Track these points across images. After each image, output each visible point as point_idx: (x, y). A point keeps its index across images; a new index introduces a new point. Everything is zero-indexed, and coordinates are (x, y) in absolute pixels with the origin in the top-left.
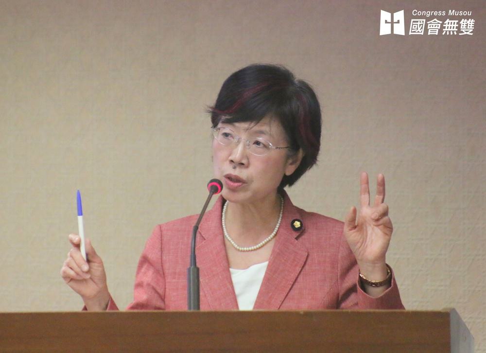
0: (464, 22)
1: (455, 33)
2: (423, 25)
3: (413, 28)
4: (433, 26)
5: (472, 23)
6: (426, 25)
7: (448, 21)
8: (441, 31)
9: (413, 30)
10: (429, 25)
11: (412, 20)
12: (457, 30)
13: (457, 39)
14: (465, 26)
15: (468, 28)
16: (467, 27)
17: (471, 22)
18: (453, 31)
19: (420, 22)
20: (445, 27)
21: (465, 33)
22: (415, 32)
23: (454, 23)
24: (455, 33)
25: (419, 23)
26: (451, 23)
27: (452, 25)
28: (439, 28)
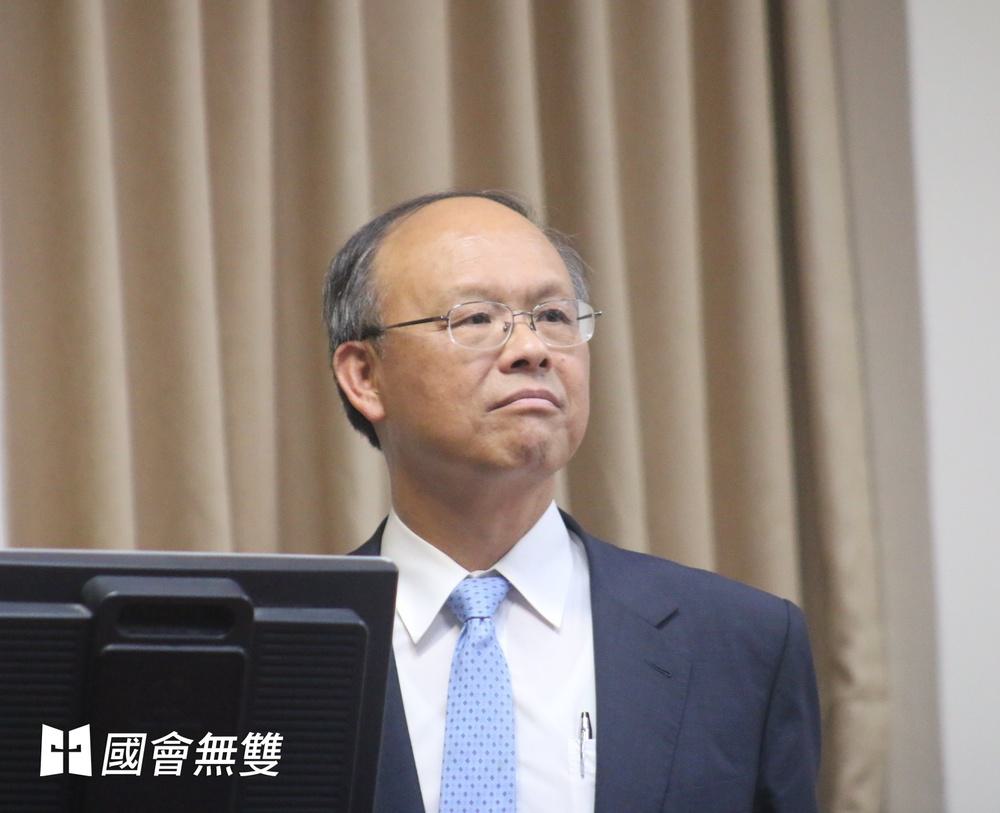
0: (252, 742)
1: (229, 772)
2: (139, 748)
3: (113, 757)
4: (167, 752)
5: (274, 744)
6: (150, 749)
7: (208, 737)
8: (189, 765)
9: (112, 764)
10: (157, 749)
11: (111, 736)
12: (233, 762)
13: (232, 787)
14: (255, 751)
15: (265, 757)
16: (261, 754)
17: (273, 741)
18: (224, 767)
19: (133, 741)
20: (200, 756)
21: (258, 771)
22: (117, 768)
23: (227, 743)
24: (229, 772)
25: (128, 744)
26: (219, 743)
27: (221, 750)
28: (184, 756)
